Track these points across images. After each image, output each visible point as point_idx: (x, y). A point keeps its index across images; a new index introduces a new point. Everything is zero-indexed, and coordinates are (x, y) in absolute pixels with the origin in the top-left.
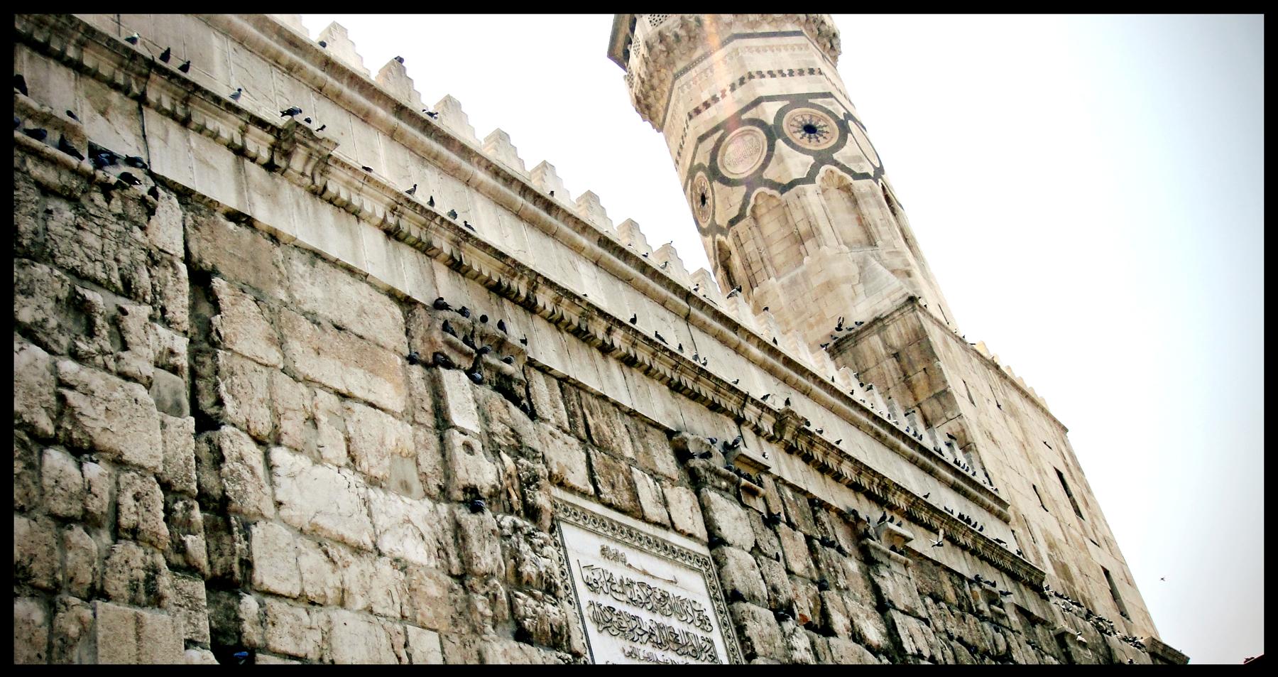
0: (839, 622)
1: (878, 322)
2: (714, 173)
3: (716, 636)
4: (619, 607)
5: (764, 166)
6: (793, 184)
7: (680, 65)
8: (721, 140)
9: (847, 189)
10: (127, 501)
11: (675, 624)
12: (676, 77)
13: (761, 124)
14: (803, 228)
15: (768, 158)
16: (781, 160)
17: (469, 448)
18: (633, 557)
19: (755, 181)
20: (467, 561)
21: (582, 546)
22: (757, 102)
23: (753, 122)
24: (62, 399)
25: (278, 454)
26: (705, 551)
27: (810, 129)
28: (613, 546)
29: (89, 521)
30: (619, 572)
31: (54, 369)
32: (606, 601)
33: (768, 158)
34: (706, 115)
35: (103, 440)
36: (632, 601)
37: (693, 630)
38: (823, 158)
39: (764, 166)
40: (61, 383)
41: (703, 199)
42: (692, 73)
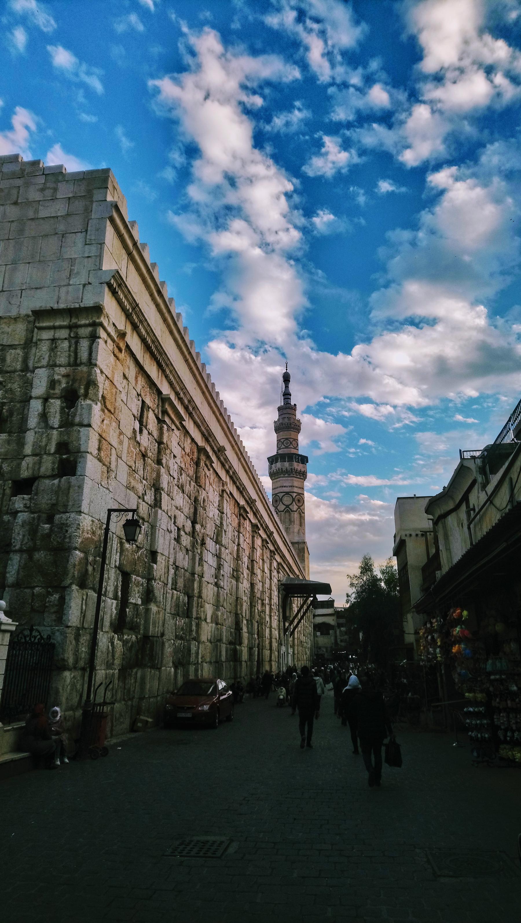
1: (298, 543)
2: (281, 500)
5: (290, 505)
6: (294, 511)
7: (282, 475)
8: (285, 495)
9: (300, 514)
12: (280, 477)
13: (292, 497)
14: (292, 520)
15: (291, 504)
16: (293, 506)
19: (287, 506)
22: (293, 492)
23: (291, 495)
27: (299, 501)
33: (291, 504)
34: (284, 488)
38: (299, 507)
39: (290, 505)
41: (276, 501)
42: (284, 479)
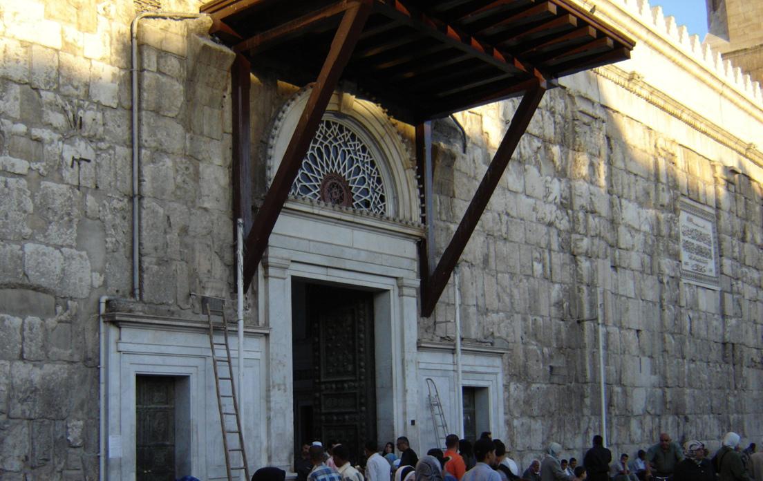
0: (749, 236)
3: (712, 248)
4: (690, 240)
10: (602, 229)
11: (702, 244)
17: (663, 188)
18: (696, 220)
20: (659, 230)
21: (683, 216)
24: (591, 198)
25: (623, 200)
26: (712, 211)
28: (691, 216)
29: (596, 236)
30: (691, 226)
31: (589, 188)
32: (686, 238)
35: (598, 210)
36: (693, 238)
37: (707, 247)
40: (591, 194)
